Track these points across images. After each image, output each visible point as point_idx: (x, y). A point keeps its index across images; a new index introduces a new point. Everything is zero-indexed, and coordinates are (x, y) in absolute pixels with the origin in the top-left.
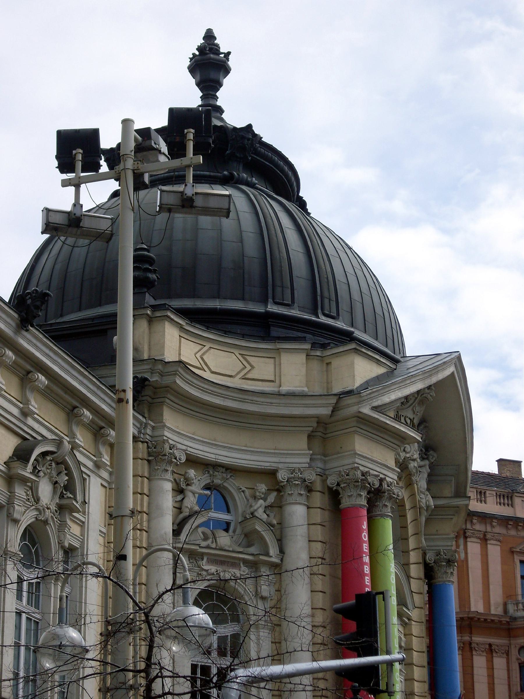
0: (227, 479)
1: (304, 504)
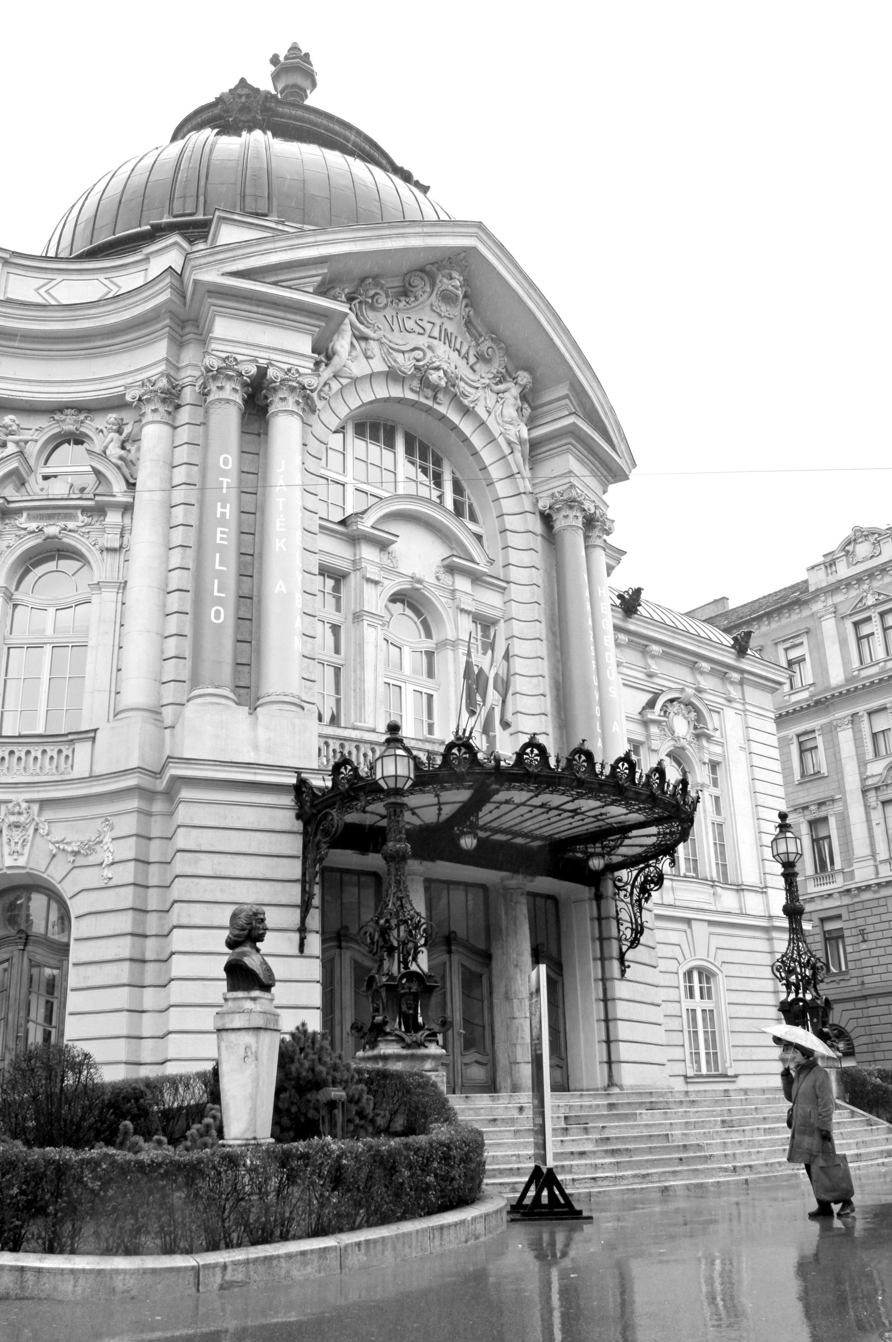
0: (82, 422)
1: (167, 423)
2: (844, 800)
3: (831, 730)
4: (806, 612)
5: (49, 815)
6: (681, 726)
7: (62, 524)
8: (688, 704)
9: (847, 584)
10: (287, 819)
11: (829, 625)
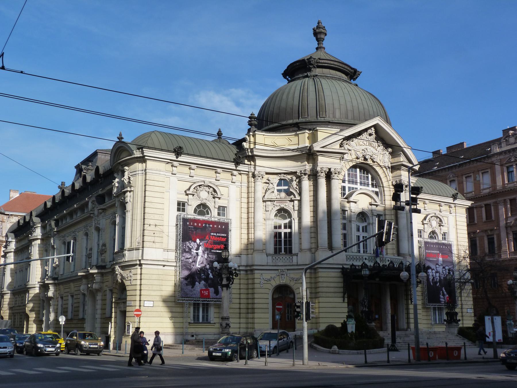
2: (499, 230)
3: (496, 205)
4: (490, 161)
5: (289, 272)
6: (435, 223)
7: (284, 204)
8: (437, 217)
9: (505, 152)
10: (339, 274)
11: (498, 168)
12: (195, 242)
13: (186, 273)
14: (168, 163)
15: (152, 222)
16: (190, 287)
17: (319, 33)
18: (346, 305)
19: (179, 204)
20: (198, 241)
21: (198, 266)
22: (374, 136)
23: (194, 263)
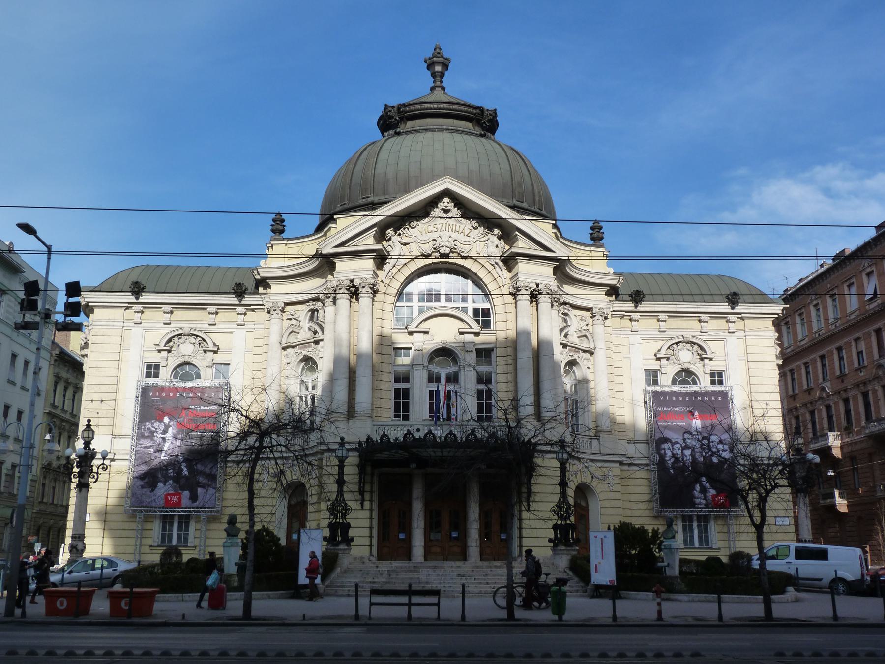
12: (161, 420)
13: (144, 468)
14: (127, 308)
15: (96, 397)
16: (147, 491)
17: (438, 65)
18: (367, 514)
19: (149, 366)
20: (166, 420)
21: (163, 457)
22: (455, 212)
23: (157, 454)
